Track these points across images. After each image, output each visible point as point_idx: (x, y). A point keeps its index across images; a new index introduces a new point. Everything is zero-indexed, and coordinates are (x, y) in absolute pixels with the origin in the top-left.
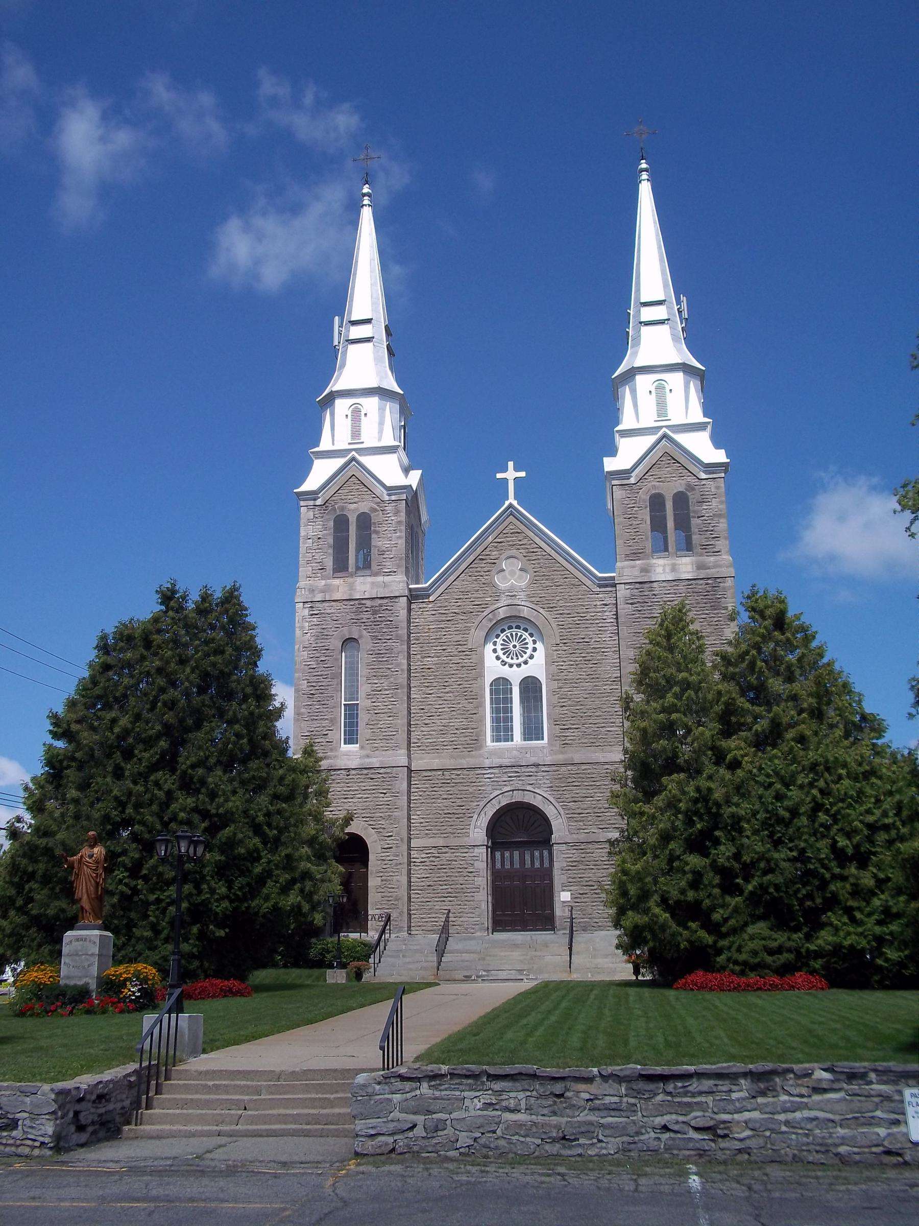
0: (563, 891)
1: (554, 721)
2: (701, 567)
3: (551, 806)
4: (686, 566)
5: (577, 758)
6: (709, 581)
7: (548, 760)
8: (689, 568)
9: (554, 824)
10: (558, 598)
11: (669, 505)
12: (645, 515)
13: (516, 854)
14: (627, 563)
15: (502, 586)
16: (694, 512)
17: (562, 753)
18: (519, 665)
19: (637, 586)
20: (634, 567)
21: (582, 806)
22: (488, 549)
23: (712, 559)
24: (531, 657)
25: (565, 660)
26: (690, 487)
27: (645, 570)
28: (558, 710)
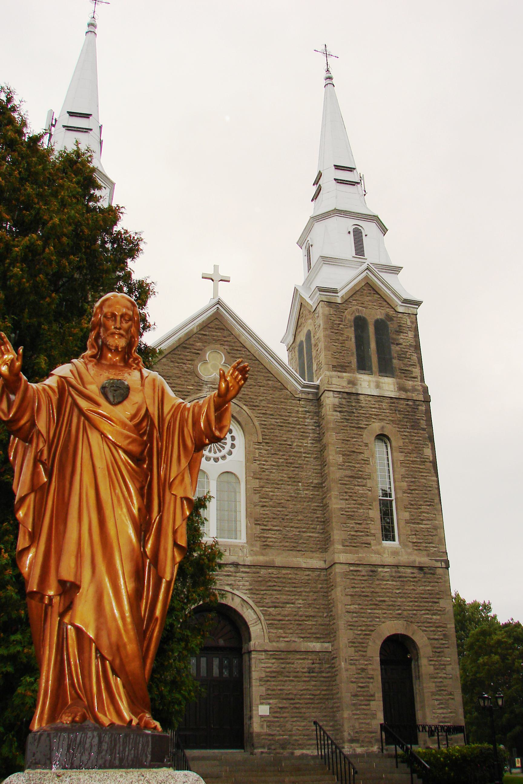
0: (262, 704)
1: (255, 520)
2: (402, 388)
3: (250, 610)
4: (389, 386)
5: (279, 560)
6: (410, 403)
7: (249, 560)
8: (392, 387)
9: (251, 629)
10: (261, 398)
11: (371, 329)
12: (351, 333)
13: (203, 660)
14: (334, 373)
15: (205, 378)
16: (393, 339)
17: (264, 555)
18: (216, 460)
19: (345, 395)
20: (343, 378)
21: (283, 613)
22: (192, 339)
23: (410, 383)
24: (230, 453)
25: (267, 459)
26: (390, 318)
27: (352, 383)
28: (258, 509)
